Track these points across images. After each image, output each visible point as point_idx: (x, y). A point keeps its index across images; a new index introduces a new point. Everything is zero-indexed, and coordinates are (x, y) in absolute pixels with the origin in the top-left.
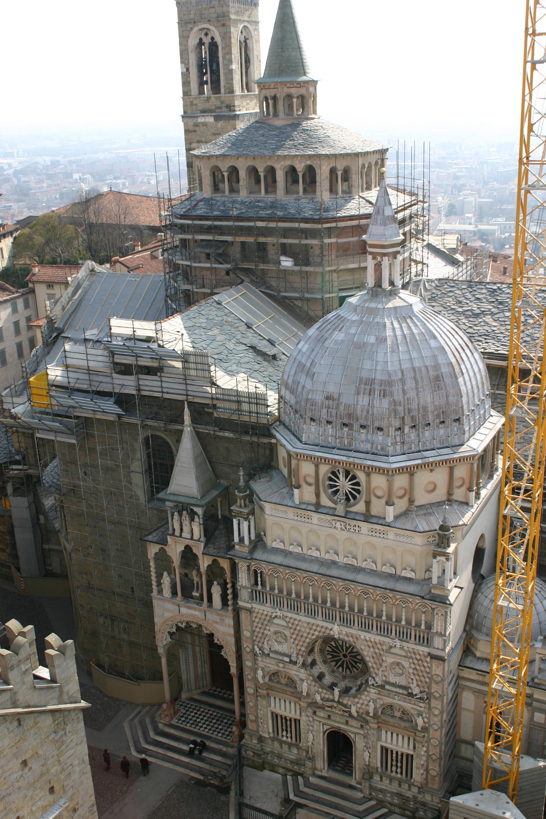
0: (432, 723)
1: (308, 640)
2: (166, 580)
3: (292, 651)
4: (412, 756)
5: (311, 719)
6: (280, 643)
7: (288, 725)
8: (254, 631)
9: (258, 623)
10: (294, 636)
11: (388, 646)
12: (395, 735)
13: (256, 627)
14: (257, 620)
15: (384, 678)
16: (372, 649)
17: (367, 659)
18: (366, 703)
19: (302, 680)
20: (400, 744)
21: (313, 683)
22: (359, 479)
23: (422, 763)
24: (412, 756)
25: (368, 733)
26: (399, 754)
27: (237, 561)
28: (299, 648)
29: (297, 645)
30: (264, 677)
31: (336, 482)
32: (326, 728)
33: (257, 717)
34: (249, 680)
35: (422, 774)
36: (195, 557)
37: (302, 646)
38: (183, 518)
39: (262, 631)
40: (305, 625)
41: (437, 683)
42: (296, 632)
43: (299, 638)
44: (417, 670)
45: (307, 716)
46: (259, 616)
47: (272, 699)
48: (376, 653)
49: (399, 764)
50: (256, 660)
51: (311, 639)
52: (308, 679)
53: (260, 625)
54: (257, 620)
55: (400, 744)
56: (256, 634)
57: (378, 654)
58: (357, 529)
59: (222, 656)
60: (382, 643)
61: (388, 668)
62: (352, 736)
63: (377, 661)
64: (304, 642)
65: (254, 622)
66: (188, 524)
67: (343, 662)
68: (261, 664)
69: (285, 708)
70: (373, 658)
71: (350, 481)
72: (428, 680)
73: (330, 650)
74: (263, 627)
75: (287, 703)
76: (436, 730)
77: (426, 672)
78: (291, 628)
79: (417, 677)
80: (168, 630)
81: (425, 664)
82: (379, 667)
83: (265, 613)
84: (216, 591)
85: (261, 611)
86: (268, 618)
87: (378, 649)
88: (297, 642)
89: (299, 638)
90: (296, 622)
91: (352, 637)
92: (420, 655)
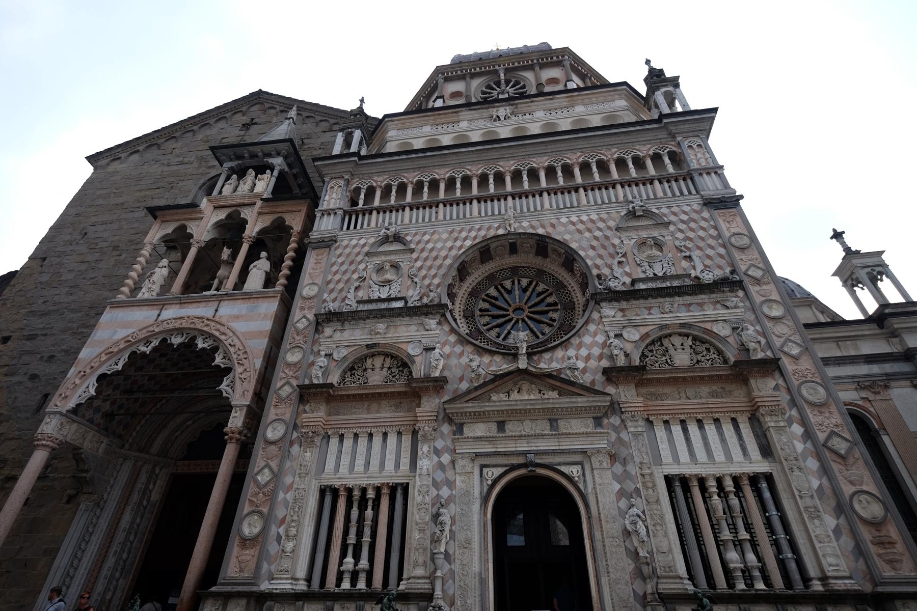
0: (778, 342)
1: (448, 262)
2: (161, 272)
3: (410, 293)
4: (769, 478)
5: (446, 459)
7: (368, 523)
8: (329, 282)
9: (343, 263)
10: (419, 264)
11: (617, 221)
12: (693, 429)
13: (336, 273)
14: (340, 260)
15: (628, 280)
16: (587, 234)
17: (582, 253)
18: (596, 351)
19: (429, 349)
20: (719, 456)
21: (458, 349)
23: (815, 483)
24: (769, 478)
25: (619, 439)
26: (729, 485)
27: (327, 179)
28: (427, 282)
29: (424, 278)
30: (326, 372)
31: (492, 93)
33: (267, 520)
34: (281, 400)
35: (837, 531)
37: (435, 276)
39: (345, 278)
41: (742, 249)
42: (425, 254)
44: (691, 239)
45: (437, 452)
46: (348, 250)
47: (334, 442)
48: (596, 238)
49: (744, 535)
50: (314, 342)
52: (444, 344)
54: (340, 260)
55: (719, 456)
56: (331, 286)
57: (602, 240)
58: (528, 116)
59: (220, 391)
60: (604, 216)
61: (630, 256)
62: (574, 471)
63: (602, 252)
64: (440, 267)
65: (333, 265)
67: (517, 321)
68: (325, 348)
69: (367, 464)
70: (593, 248)
71: (512, 87)
72: (722, 251)
73: (486, 306)
74: (353, 267)
75: (377, 440)
76: (795, 358)
77: (712, 237)
78: (412, 251)
79: (698, 252)
80: (103, 370)
81: (704, 224)
82: (609, 261)
83: (362, 242)
84: (261, 268)
85: (354, 242)
86: (366, 249)
87: (600, 229)
88: (423, 272)
89: (429, 263)
90: (427, 237)
91: (543, 226)
92: (685, 213)
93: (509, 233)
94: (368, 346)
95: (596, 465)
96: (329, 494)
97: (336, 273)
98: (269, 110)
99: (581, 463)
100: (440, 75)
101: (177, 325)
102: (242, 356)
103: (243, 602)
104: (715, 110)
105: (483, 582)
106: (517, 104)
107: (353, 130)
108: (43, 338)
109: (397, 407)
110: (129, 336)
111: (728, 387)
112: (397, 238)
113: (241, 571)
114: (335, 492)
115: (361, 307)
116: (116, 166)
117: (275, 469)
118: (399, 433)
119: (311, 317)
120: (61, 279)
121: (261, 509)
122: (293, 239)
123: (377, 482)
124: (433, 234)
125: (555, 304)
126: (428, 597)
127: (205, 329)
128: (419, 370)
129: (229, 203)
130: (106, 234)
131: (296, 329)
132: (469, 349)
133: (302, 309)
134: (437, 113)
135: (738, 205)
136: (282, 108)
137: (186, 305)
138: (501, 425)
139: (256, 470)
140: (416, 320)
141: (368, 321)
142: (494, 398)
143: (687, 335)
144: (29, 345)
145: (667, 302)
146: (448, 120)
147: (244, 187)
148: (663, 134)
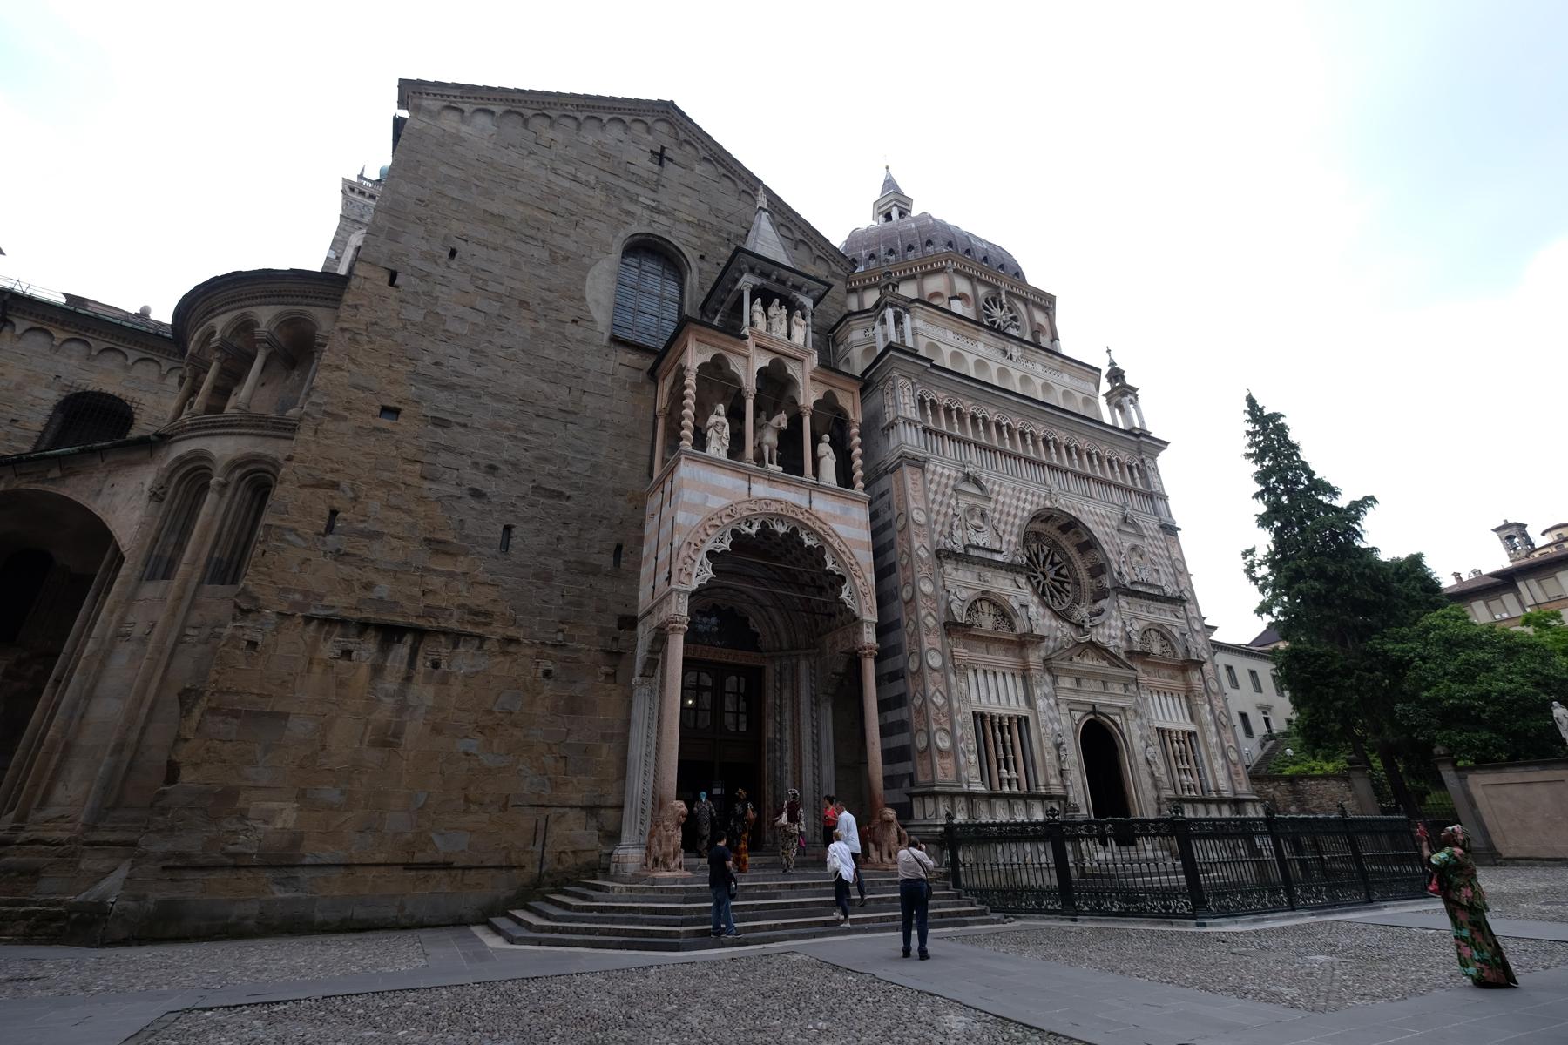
1: (1018, 521)
4: (1195, 733)
5: (1052, 701)
6: (978, 529)
9: (936, 493)
10: (997, 515)
13: (934, 501)
14: (934, 487)
22: (1018, 311)
32: (1078, 715)
33: (951, 734)
36: (790, 382)
37: (1011, 533)
38: (773, 310)
39: (943, 510)
40: (1010, 492)
43: (1004, 518)
44: (1155, 555)
45: (1046, 696)
47: (971, 674)
51: (1021, 518)
53: (939, 498)
58: (1029, 364)
60: (1110, 515)
62: (1117, 719)
64: (1013, 524)
66: (785, 322)
75: (999, 677)
80: (709, 546)
83: (946, 472)
86: (951, 482)
89: (1004, 518)
93: (1057, 509)
94: (984, 592)
95: (1129, 717)
96: (979, 717)
97: (934, 501)
98: (684, 144)
99: (1119, 715)
100: (950, 262)
101: (773, 508)
102: (857, 568)
103: (963, 799)
104: (1167, 443)
105: (1084, 787)
106: (1025, 348)
107: (902, 311)
108: (462, 430)
109: (1006, 650)
110: (727, 508)
111: (1177, 673)
112: (976, 482)
113: (946, 776)
114: (983, 716)
115: (972, 552)
116: (450, 122)
117: (945, 694)
118: (1013, 675)
119: (928, 546)
120: (447, 327)
121: (944, 726)
122: (855, 430)
123: (1012, 713)
124: (1001, 485)
125: (1066, 577)
126: (1065, 798)
127: (809, 523)
128: (1021, 626)
129: (774, 347)
130: (496, 270)
131: (918, 555)
132: (1048, 612)
133: (917, 535)
134: (966, 323)
135: (1176, 535)
136: (707, 155)
137: (775, 484)
138: (1078, 680)
139: (931, 693)
140: (1011, 575)
141: (976, 566)
142: (1075, 659)
143: (1158, 632)
144: (442, 436)
145: (1154, 605)
146: (964, 332)
147: (780, 330)
148: (1134, 447)
